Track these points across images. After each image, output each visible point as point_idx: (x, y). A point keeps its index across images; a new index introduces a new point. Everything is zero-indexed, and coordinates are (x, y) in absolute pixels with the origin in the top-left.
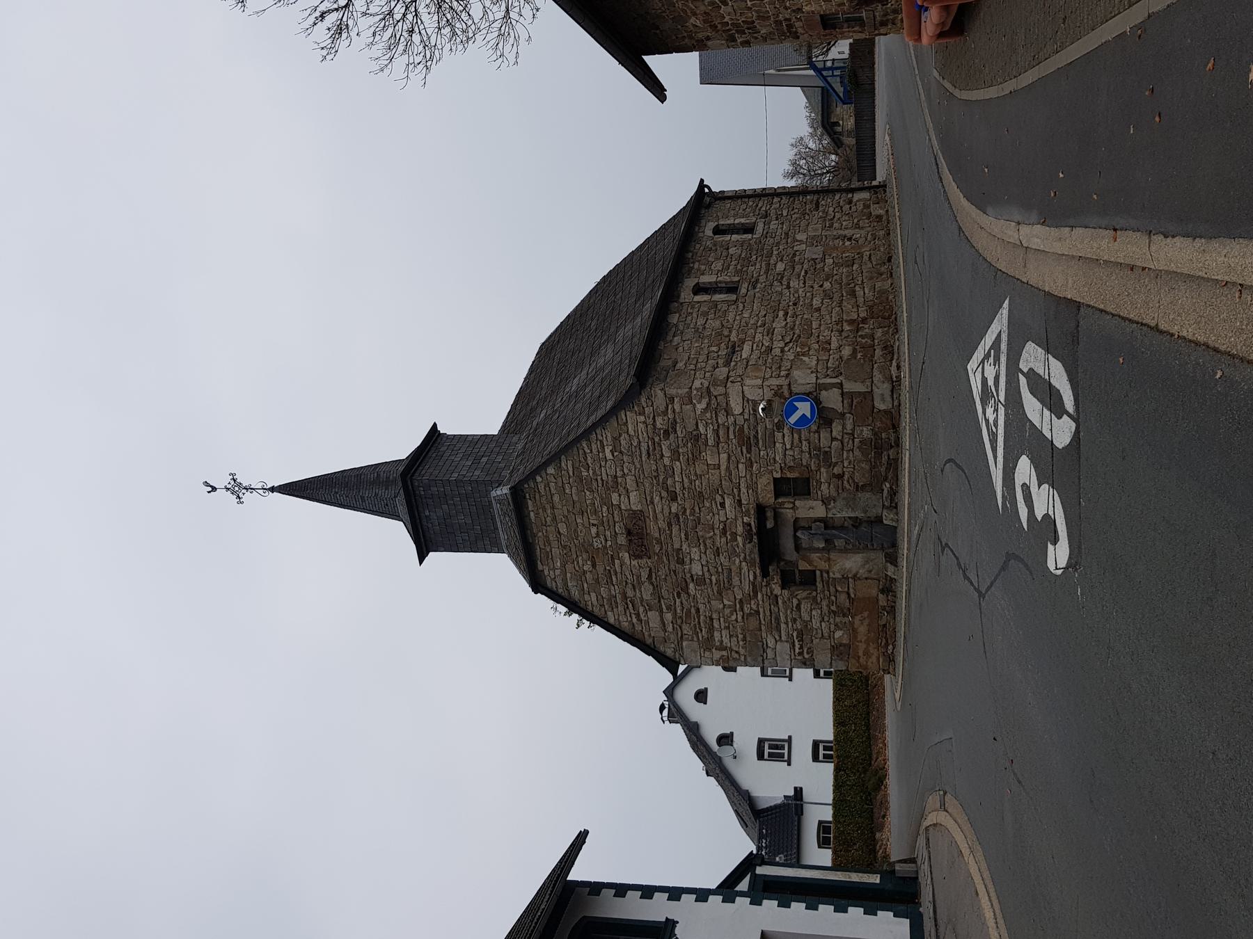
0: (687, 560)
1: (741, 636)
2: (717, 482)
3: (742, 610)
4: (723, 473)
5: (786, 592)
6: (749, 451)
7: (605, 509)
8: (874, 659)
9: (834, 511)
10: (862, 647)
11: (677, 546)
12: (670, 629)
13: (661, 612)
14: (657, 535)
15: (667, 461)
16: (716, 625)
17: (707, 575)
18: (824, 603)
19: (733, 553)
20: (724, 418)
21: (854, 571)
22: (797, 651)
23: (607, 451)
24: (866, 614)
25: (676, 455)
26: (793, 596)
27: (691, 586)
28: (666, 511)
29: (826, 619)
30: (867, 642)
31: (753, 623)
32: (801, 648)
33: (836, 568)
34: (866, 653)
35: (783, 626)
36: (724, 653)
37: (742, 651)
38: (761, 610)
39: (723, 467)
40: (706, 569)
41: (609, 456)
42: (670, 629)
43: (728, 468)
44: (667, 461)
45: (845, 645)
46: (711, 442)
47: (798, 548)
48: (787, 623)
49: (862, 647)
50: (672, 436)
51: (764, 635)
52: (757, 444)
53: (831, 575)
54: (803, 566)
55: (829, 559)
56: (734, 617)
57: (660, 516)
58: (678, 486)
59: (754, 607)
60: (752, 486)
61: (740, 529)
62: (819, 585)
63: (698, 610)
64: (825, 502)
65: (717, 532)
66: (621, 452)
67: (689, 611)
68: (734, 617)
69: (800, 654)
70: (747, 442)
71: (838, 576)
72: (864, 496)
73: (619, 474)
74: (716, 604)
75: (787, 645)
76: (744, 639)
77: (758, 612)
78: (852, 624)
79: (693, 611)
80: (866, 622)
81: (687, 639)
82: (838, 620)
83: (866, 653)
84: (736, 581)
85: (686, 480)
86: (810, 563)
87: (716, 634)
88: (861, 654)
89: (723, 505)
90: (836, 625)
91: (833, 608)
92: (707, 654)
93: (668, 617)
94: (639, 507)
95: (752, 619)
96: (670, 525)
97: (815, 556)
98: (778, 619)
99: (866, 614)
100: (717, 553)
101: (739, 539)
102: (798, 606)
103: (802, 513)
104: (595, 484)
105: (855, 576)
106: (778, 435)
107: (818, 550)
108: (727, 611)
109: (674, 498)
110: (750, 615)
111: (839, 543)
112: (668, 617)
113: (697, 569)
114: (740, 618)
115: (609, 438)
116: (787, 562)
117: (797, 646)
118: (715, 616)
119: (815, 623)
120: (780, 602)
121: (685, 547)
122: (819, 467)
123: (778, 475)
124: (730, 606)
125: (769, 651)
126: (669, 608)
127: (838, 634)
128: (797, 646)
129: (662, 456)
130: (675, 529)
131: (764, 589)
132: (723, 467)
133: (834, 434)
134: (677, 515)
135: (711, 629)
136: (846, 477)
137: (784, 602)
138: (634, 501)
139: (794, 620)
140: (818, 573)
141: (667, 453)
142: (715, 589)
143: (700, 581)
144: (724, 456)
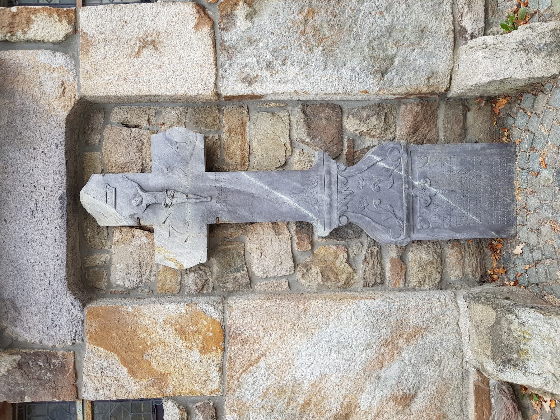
9: (247, 60)
47: (85, 280)
55: (223, 334)
86: (133, 354)
97: (156, 318)
103: (106, 74)
107: (172, 287)
111: (267, 252)
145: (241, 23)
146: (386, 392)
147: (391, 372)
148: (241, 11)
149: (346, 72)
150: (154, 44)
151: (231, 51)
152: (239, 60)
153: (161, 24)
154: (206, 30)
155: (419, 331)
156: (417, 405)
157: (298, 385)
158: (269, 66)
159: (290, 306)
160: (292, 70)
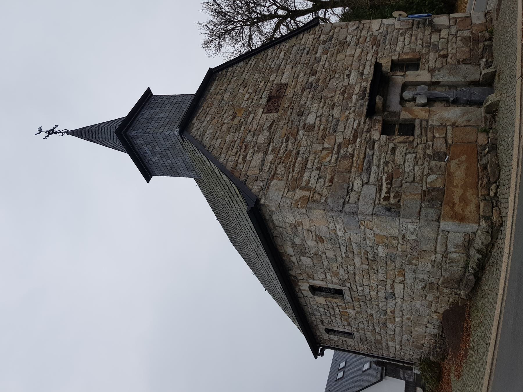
3: (338, 152)
5: (384, 138)
8: (472, 207)
12: (266, 168)
16: (309, 166)
18: (421, 147)
20: (366, 33)
22: (383, 194)
24: (464, 158)
25: (326, 52)
26: (390, 141)
27: (301, 132)
29: (420, 162)
31: (344, 164)
32: (388, 192)
34: (464, 200)
35: (374, 168)
36: (307, 194)
37: (325, 192)
38: (356, 153)
40: (318, 119)
45: (438, 190)
48: (378, 166)
50: (327, 43)
51: (352, 177)
53: (430, 122)
54: (405, 115)
55: (430, 111)
59: (350, 150)
62: (417, 131)
63: (298, 153)
67: (290, 153)
68: (328, 159)
71: (436, 123)
72: (464, 68)
77: (352, 156)
78: (447, 168)
79: (294, 152)
80: (464, 166)
82: (433, 163)
83: (464, 200)
87: (307, 174)
88: (456, 200)
90: (430, 169)
91: (429, 152)
99: (464, 158)
101: (354, 97)
102: (394, 149)
106: (401, 39)
109: (314, 73)
114: (334, 159)
116: (392, 113)
117: (384, 190)
118: (311, 157)
119: (408, 167)
120: (376, 146)
122: (428, 52)
124: (328, 149)
125: (353, 194)
126: (273, 150)
128: (384, 190)
130: (306, 93)
131: (364, 135)
133: (442, 36)
135: (303, 169)
136: (450, 56)
137: (380, 146)
139: (387, 163)
140: (417, 121)
142: (321, 134)
144: (359, 50)
157: (445, 118)
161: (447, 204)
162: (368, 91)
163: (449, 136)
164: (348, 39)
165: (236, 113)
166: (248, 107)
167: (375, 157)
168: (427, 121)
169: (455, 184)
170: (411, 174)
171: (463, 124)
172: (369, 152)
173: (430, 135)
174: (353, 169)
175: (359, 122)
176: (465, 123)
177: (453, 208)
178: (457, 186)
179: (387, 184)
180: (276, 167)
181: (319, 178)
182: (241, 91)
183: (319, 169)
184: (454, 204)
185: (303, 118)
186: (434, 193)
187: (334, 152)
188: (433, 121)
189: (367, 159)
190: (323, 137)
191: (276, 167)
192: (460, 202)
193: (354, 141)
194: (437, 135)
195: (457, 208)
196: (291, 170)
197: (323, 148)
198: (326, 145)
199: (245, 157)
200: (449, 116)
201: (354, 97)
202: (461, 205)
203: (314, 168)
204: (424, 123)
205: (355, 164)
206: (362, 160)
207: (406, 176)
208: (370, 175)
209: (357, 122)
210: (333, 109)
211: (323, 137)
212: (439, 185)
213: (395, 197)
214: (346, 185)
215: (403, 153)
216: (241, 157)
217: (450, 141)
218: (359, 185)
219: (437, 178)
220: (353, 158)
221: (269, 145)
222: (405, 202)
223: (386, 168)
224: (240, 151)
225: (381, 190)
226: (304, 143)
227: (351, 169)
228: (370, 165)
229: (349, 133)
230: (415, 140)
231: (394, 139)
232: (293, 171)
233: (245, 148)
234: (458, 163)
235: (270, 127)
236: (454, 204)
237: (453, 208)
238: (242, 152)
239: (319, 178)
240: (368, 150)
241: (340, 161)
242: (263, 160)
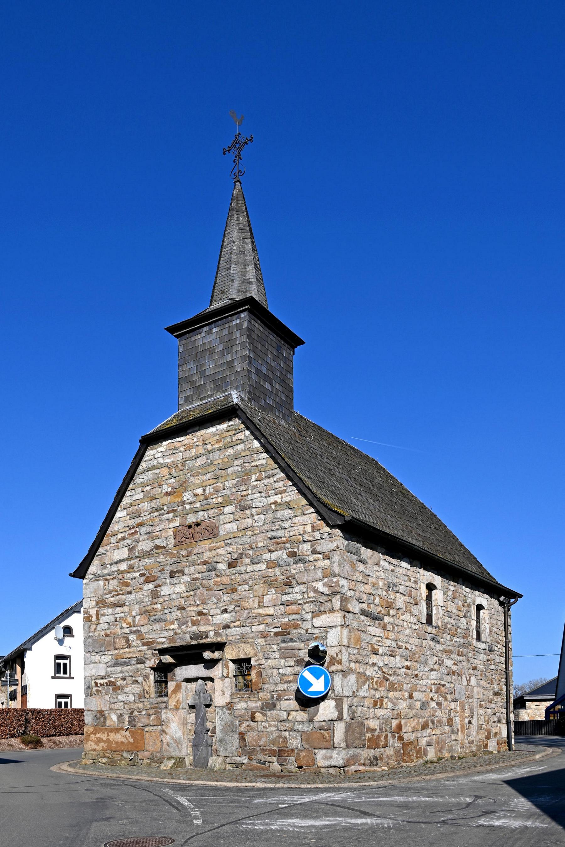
0: (175, 580)
1: (108, 632)
2: (246, 605)
3: (132, 632)
4: (256, 611)
6: (276, 634)
7: (220, 500)
9: (221, 713)
10: (104, 736)
11: (186, 570)
13: (128, 559)
14: (196, 551)
15: (267, 556)
17: (161, 600)
18: (140, 706)
19: (182, 622)
21: (167, 731)
23: (278, 498)
24: (131, 740)
27: (151, 586)
28: (218, 559)
29: (126, 706)
30: (108, 741)
31: (121, 643)
33: (170, 715)
34: (99, 741)
35: (119, 669)
36: (94, 618)
37: (96, 634)
38: (131, 650)
39: (261, 611)
41: (271, 500)
42: (114, 568)
43: (260, 615)
44: (267, 556)
45: (104, 722)
46: (286, 598)
48: (122, 672)
49: (104, 736)
50: (291, 560)
52: (283, 641)
56: (124, 625)
57: (214, 553)
58: (243, 569)
60: (243, 639)
61: (203, 629)
63: (129, 593)
64: (229, 706)
65: (200, 608)
66: (275, 511)
67: (128, 585)
68: (124, 625)
69: (96, 684)
70: (284, 634)
71: (163, 717)
73: (254, 511)
74: (136, 609)
75: (103, 673)
76: (107, 635)
77: (129, 646)
78: (122, 729)
79: (129, 589)
80: (124, 740)
81: (105, 585)
84: (157, 626)
85: (248, 576)
87: (110, 611)
88: (98, 735)
89: (225, 611)
91: (135, 713)
92: (94, 603)
93: (123, 566)
94: (222, 533)
95: (124, 641)
96: (205, 563)
98: (125, 664)
99: (131, 740)
100: (181, 608)
101: (194, 628)
102: (137, 682)
104: (243, 488)
105: (164, 731)
108: (130, 620)
110: (127, 640)
112: (123, 566)
113: (165, 590)
115: (288, 499)
117: (102, 681)
118: (126, 609)
119: (122, 697)
121: (187, 578)
123: (253, 662)
124: (134, 621)
125: (98, 657)
127: (114, 717)
129: (271, 551)
132: (261, 611)
134: (214, 569)
138: (227, 528)
139: (124, 679)
140: (166, 699)
141: (274, 556)
142: (149, 608)
143: (155, 594)
144: (271, 611)
145: (227, 712)
146: (169, 740)
147: (172, 742)
148: (229, 712)
149: (220, 734)
150: (223, 694)
151: (222, 710)
152: (220, 711)
153: (226, 695)
154: (225, 704)
155: (178, 747)
156: (167, 747)
158: (220, 718)
159: (181, 722)
160: (219, 722)
161: (95, 730)
162: (202, 641)
163: (151, 728)
164: (298, 589)
165: (175, 492)
166: (184, 503)
167: (129, 667)
168: (166, 708)
169: (110, 734)
170: (116, 700)
171: (163, 739)
172: (134, 661)
173: (151, 712)
174: (116, 651)
175: (164, 643)
176: (165, 741)
177: (92, 733)
178: (108, 735)
179: (106, 683)
180: (114, 578)
181: (109, 623)
182: (208, 476)
183: (116, 621)
184: (95, 734)
185: (168, 581)
186: (102, 720)
187: (132, 628)
188: (165, 713)
189: (127, 660)
190: (146, 612)
191: (114, 578)
192: (97, 738)
193: (144, 644)
194: (152, 718)
195: (92, 736)
196: (113, 594)
197: (135, 617)
198: (137, 618)
199: (123, 539)
200: (172, 727)
201: (194, 628)
202: (95, 739)
203: (116, 616)
204: (164, 705)
205: (121, 651)
206: (126, 656)
207: (114, 696)
208: (114, 667)
209: (164, 640)
210: (178, 610)
211: (146, 612)
212: (108, 723)
213: (97, 691)
214: (103, 649)
215: (133, 691)
216: (123, 535)
217: (147, 729)
218: (104, 660)
219: (114, 721)
220: (127, 648)
221: (137, 557)
222: (94, 699)
223: (119, 679)
224: (130, 529)
225: (102, 678)
226: (139, 595)
227: (117, 649)
228: (123, 665)
229: (150, 636)
230: (146, 700)
231: (145, 681)
232: (112, 597)
233: (132, 533)
234: (127, 736)
235: (157, 547)
236: (95, 734)
237: (92, 733)
238: (127, 533)
239: (109, 623)
240: (135, 659)
241: (123, 637)
242: (121, 561)
